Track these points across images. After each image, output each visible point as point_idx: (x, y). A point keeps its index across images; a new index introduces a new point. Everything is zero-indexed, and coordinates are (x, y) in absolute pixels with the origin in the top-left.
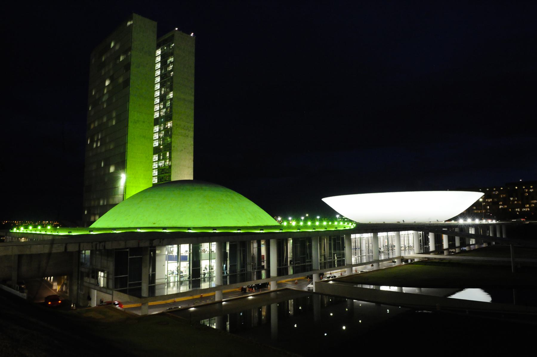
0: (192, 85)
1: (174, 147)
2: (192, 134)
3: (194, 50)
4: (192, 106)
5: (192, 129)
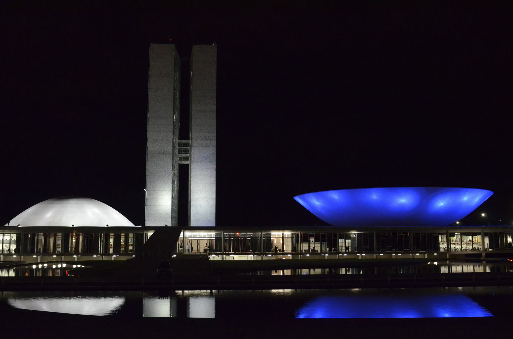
0: (214, 94)
1: (194, 158)
2: (214, 143)
3: (215, 59)
4: (214, 116)
5: (214, 138)
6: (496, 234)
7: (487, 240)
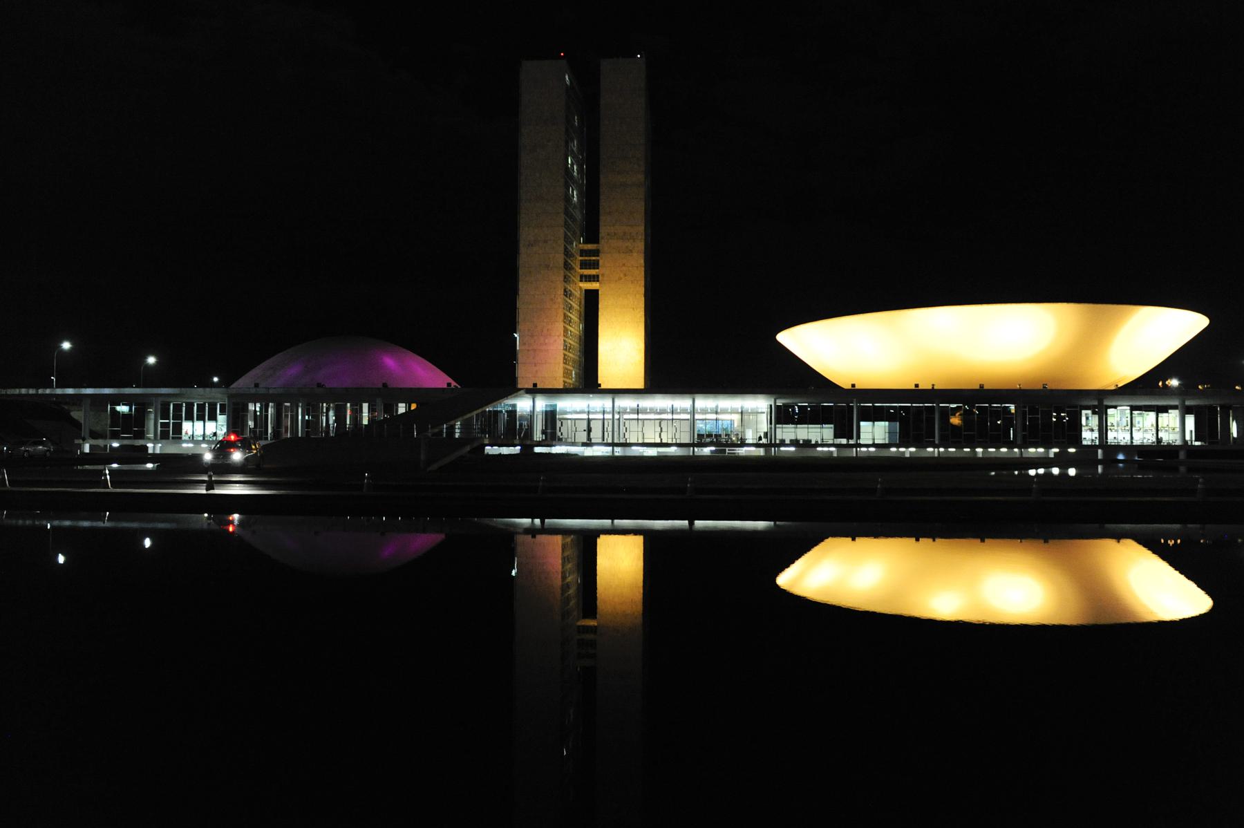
2: (641, 245)
6: (1212, 409)
7: (1190, 421)
